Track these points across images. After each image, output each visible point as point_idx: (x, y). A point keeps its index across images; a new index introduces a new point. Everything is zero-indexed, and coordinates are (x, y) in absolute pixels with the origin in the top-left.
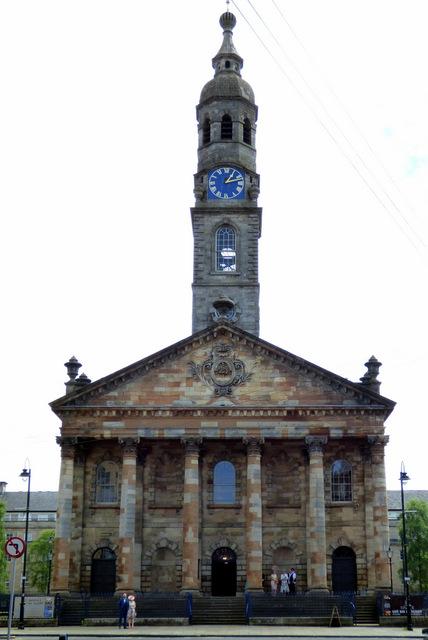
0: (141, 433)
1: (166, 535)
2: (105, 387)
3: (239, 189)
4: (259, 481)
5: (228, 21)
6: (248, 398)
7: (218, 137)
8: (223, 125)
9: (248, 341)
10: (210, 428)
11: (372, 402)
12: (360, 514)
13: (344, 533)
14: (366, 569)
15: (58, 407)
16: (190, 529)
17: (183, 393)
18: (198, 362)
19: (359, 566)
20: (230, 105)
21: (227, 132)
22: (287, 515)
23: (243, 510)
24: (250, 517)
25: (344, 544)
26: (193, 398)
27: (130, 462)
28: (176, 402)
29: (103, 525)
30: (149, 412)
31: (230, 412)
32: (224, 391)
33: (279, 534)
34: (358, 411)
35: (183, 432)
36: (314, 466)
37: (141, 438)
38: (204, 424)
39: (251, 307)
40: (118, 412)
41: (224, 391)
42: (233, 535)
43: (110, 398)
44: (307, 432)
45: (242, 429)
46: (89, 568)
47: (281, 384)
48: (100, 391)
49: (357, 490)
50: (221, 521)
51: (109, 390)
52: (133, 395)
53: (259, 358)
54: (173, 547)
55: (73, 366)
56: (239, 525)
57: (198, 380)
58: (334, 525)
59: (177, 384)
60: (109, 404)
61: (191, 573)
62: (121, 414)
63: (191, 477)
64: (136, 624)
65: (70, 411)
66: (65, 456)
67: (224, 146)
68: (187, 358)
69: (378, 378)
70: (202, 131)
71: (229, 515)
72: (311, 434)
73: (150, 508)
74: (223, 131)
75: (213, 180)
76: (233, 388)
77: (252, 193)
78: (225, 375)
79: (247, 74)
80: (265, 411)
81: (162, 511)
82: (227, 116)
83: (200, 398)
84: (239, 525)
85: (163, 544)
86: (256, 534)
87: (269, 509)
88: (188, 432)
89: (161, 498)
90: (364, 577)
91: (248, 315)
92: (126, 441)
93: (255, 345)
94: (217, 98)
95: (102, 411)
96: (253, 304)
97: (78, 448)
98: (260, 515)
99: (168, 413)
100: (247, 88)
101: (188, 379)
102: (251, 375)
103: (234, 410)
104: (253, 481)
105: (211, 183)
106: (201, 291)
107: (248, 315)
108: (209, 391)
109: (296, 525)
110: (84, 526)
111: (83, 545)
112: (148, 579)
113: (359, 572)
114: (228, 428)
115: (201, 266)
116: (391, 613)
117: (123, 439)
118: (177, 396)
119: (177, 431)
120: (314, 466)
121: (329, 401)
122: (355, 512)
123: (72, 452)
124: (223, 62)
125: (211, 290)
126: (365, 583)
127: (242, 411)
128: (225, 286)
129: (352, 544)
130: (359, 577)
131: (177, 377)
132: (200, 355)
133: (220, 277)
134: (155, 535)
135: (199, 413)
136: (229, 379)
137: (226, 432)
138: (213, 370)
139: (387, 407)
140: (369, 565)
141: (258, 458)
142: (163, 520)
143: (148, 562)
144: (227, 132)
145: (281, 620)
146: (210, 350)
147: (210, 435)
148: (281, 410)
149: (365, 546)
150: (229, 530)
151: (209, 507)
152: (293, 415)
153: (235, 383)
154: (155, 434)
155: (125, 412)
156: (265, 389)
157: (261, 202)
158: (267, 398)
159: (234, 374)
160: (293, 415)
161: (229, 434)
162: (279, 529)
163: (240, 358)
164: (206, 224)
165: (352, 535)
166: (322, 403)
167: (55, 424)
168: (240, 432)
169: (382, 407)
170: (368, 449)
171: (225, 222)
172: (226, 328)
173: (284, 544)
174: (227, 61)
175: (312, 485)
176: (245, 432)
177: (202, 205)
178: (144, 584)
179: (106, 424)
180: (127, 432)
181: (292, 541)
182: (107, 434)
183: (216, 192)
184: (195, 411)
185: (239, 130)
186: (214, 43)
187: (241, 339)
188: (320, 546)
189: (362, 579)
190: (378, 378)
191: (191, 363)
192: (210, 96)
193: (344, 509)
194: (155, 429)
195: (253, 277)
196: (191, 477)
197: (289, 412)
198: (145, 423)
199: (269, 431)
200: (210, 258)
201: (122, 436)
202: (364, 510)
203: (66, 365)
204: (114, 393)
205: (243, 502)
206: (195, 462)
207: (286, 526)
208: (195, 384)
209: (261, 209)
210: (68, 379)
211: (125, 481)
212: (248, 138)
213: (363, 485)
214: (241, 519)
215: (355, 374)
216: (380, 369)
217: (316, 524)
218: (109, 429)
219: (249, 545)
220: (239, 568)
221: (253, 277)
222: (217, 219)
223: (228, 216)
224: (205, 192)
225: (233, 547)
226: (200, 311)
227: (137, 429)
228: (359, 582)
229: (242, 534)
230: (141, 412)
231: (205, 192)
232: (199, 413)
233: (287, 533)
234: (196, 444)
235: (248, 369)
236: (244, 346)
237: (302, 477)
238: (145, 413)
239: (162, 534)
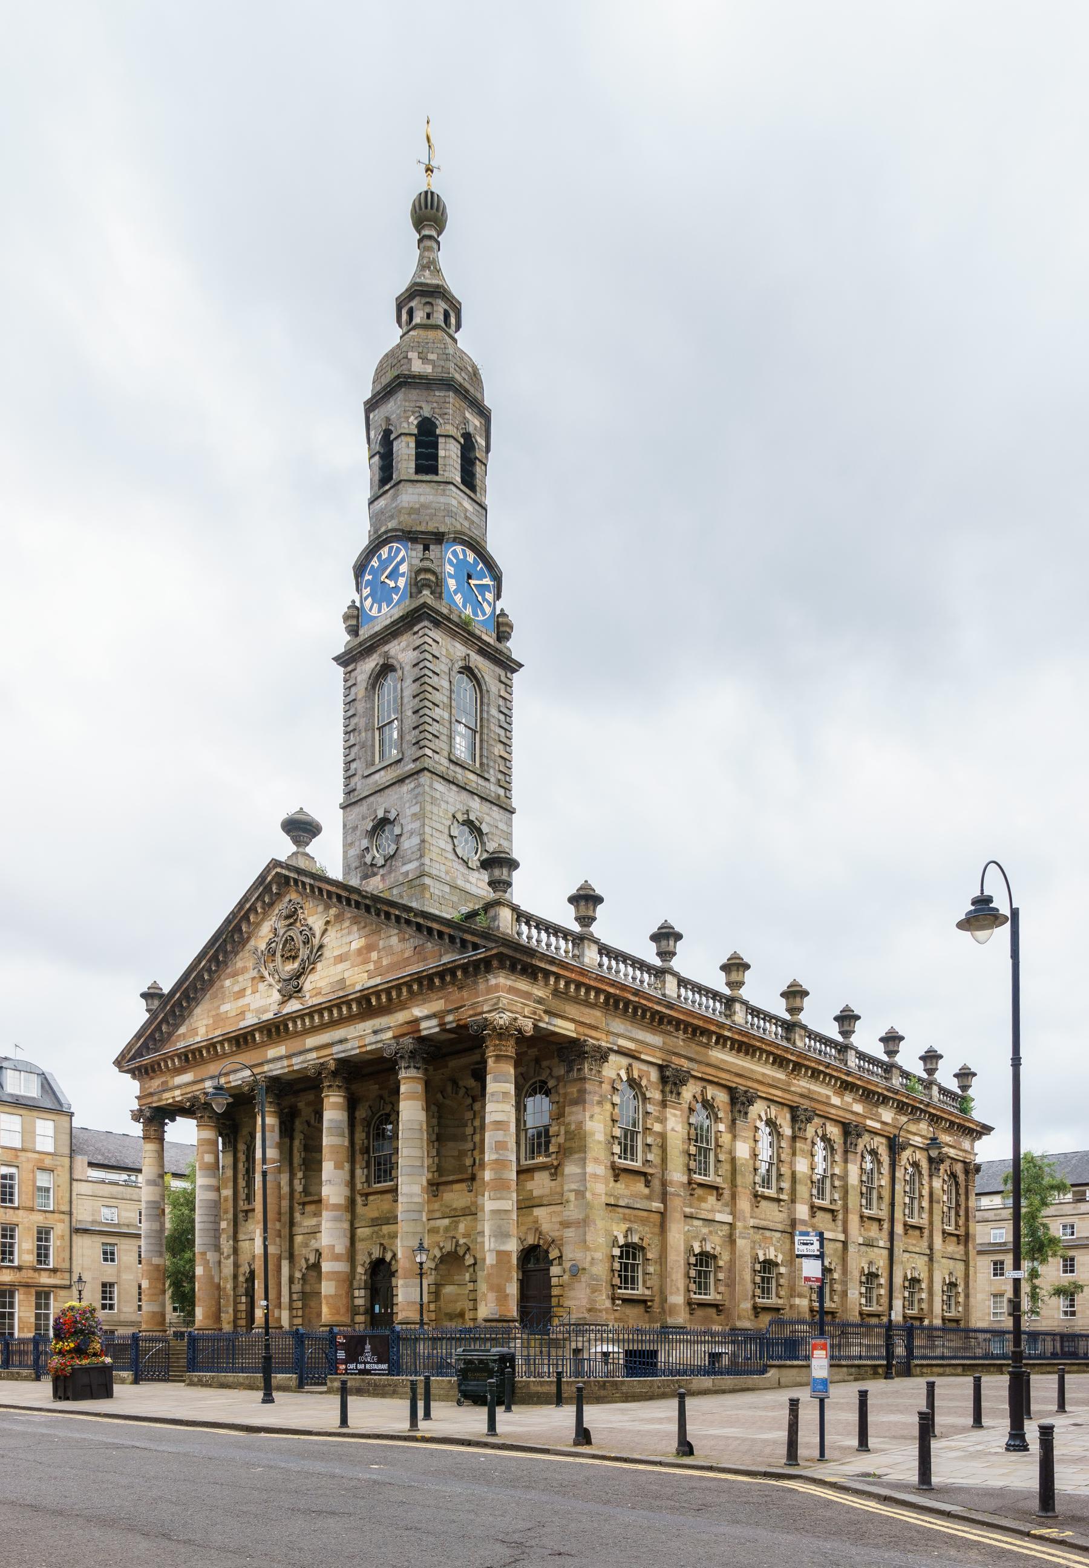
22: (456, 1197)
32: (292, 988)
33: (447, 1229)
41: (292, 988)
50: (375, 1214)
137: (295, 1060)
147: (276, 1069)
151: (362, 1195)
162: (446, 1221)
184: (252, 1033)
188: (497, 1242)
193: (538, 1175)
207: (456, 1215)
233: (456, 1228)
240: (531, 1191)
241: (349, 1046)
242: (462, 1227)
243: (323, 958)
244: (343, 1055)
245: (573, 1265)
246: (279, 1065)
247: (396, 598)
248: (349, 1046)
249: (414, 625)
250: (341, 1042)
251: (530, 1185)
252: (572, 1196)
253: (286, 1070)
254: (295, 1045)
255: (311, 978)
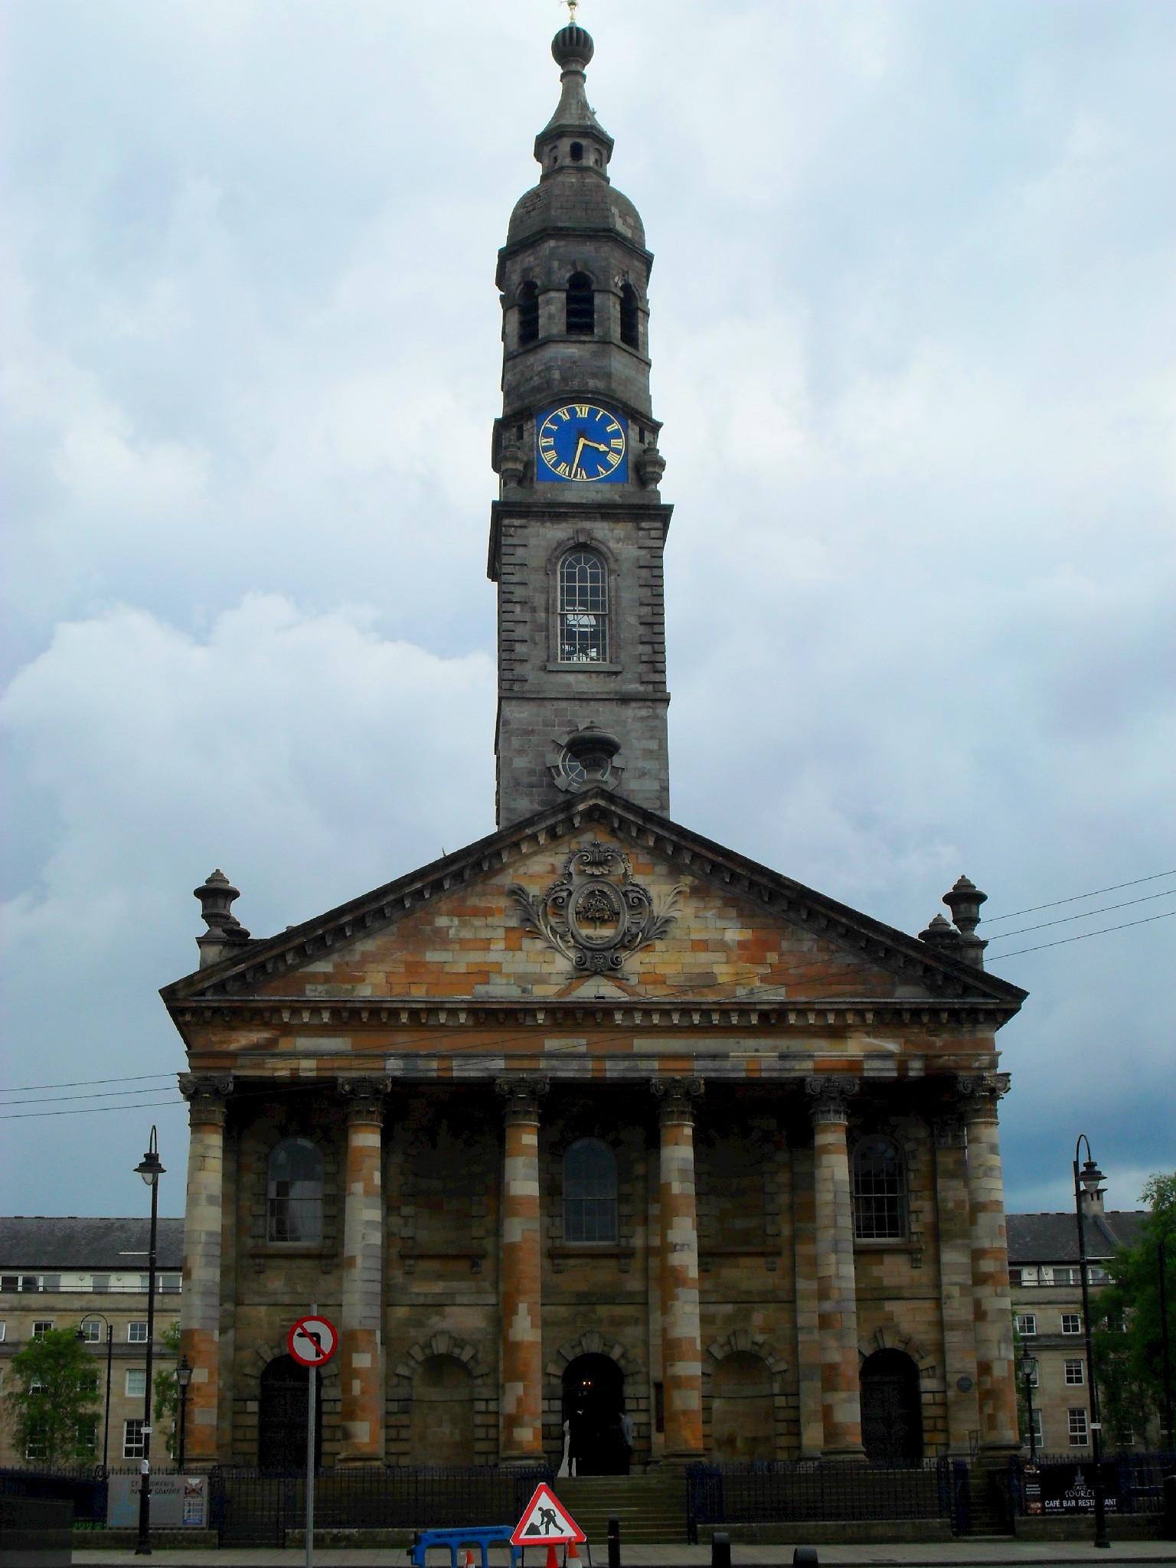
0: (394, 1066)
1: (445, 1325)
2: (300, 951)
3: (614, 460)
4: (691, 1188)
5: (572, 48)
6: (661, 981)
7: (559, 326)
8: (570, 300)
9: (659, 839)
10: (567, 1056)
11: (967, 990)
12: (922, 1275)
13: (890, 1318)
14: (944, 1404)
15: (180, 1000)
16: (523, 1308)
17: (499, 964)
18: (534, 890)
19: (926, 1398)
20: (587, 252)
21: (580, 318)
22: (748, 1275)
23: (637, 1263)
24: (671, 1278)
25: (889, 1342)
26: (524, 980)
27: (367, 1139)
28: (481, 990)
29: (287, 1299)
30: (414, 1013)
31: (618, 1017)
33: (729, 1319)
34: (934, 1012)
35: (501, 1064)
36: (826, 1149)
37: (395, 1080)
38: (552, 1044)
39: (648, 753)
40: (335, 1012)
41: (596, 962)
42: (618, 1323)
43: (314, 978)
44: (809, 1065)
45: (651, 1056)
46: (253, 1406)
47: (742, 945)
48: (290, 959)
49: (919, 1212)
50: (582, 1287)
51: (310, 959)
52: (376, 974)
53: (687, 881)
54: (466, 1355)
55: (215, 895)
56: (629, 1298)
57: (535, 934)
58: (870, 1296)
59: (486, 945)
60: (314, 992)
61: (527, 1418)
62: (347, 1016)
63: (523, 1180)
64: (319, 1543)
65: (216, 1011)
66: (197, 1124)
67: (572, 351)
68: (507, 880)
69: (979, 932)
70: (515, 317)
71: (603, 1274)
72: (815, 1070)
73: (403, 1257)
74: (570, 313)
75: (548, 433)
76: (624, 955)
77: (646, 468)
78: (603, 921)
79: (620, 174)
80: (706, 1013)
81: (434, 1265)
82: (573, 278)
83: (541, 980)
84: (629, 1298)
85: (441, 1347)
86: (687, 1319)
87: (706, 1256)
88: (516, 1064)
89: (751, 1222)
90: (940, 1424)
91: (643, 774)
92: (357, 1084)
93: (678, 849)
94: (559, 233)
95: (295, 1011)
96: (653, 745)
97: (241, 1109)
98: (693, 1272)
99: (462, 1018)
100: (628, 210)
101: (508, 929)
102: (667, 921)
103: (628, 1009)
104: (676, 1188)
105: (544, 442)
106: (521, 713)
107: (643, 774)
108: (563, 963)
109: (766, 1298)
110: (238, 1303)
111: (238, 1348)
112: (404, 1434)
113: (927, 1412)
114: (612, 1057)
115: (518, 647)
116: (1043, 1508)
117: (352, 1081)
118: (483, 974)
119: (485, 1061)
120: (826, 1149)
121: (860, 988)
122: (915, 1263)
123: (219, 1114)
124: (565, 145)
125: (548, 711)
126: (940, 1438)
127: (647, 1013)
128: (582, 699)
129: (907, 1342)
130: (927, 1424)
131: (477, 928)
132: (537, 870)
133: (570, 678)
134: (420, 1324)
135: (541, 1018)
136: (611, 927)
137: (608, 1064)
138: (571, 910)
139: (1006, 1000)
140: (951, 1394)
141: (688, 1131)
142: (438, 1287)
143: (402, 1392)
144: (580, 318)
145: (880, 1527)
146: (563, 858)
147: (568, 1071)
148: (744, 1009)
149: (940, 1349)
150: (603, 1311)
152: (771, 1020)
153: (627, 943)
154: (431, 1068)
155: (355, 1013)
156: (703, 957)
157: (667, 490)
158: (708, 980)
159: (626, 919)
160: (771, 1020)
161: (614, 1070)
162: (729, 1308)
163: (638, 879)
164: (533, 542)
165: (910, 1320)
166: (846, 995)
167: (170, 1053)
168: (644, 1064)
169: (991, 1003)
170: (940, 1105)
171: (582, 539)
172: (602, 803)
173: (743, 1344)
174: (573, 144)
175: (825, 1196)
176: (656, 1065)
177: (518, 495)
178: (395, 1448)
179: (303, 1043)
180: (355, 1063)
181: (760, 1339)
182: (308, 1068)
183: (556, 465)
185: (608, 308)
186: (540, 96)
187: (641, 831)
189: (935, 1430)
190: (979, 932)
191: (517, 894)
192: (531, 232)
193: (888, 1259)
194: (429, 1056)
195: (657, 677)
196: (523, 1180)
197: (764, 1015)
198: (403, 1041)
199: (717, 1064)
200: (546, 628)
201: (347, 1073)
202: (937, 1260)
203: (199, 893)
204: (323, 967)
205: (638, 1242)
206: (530, 1139)
207: (746, 1301)
208: (527, 943)
209: (669, 509)
210: (203, 928)
211: (358, 1187)
212: (632, 334)
213: (934, 1198)
214: (634, 1284)
215: (913, 913)
216: (984, 910)
217: (835, 1294)
218: (309, 1054)
219: (671, 1349)
220: (630, 1405)
221: (657, 677)
222: (558, 532)
223: (588, 525)
224: (528, 465)
225: (616, 1354)
226: (521, 763)
227: (385, 1056)
228: (926, 1437)
229: (636, 1321)
230: (394, 1013)
231: (528, 465)
232: (541, 1018)
234: (687, 1093)
235: (660, 908)
236: (650, 851)
237: (783, 1178)
238: (404, 1018)
239: (436, 1322)
240: (880, 1279)
241: (728, 1064)
242: (758, 1318)
243: (670, 936)
244: (713, 1075)
245: (962, 1379)
246: (574, 1064)
247: (604, 473)
248: (728, 1064)
249: (643, 520)
250: (714, 1057)
251: (876, 1271)
252: (956, 1291)
253: (589, 1075)
254: (606, 1043)
255: (639, 956)
